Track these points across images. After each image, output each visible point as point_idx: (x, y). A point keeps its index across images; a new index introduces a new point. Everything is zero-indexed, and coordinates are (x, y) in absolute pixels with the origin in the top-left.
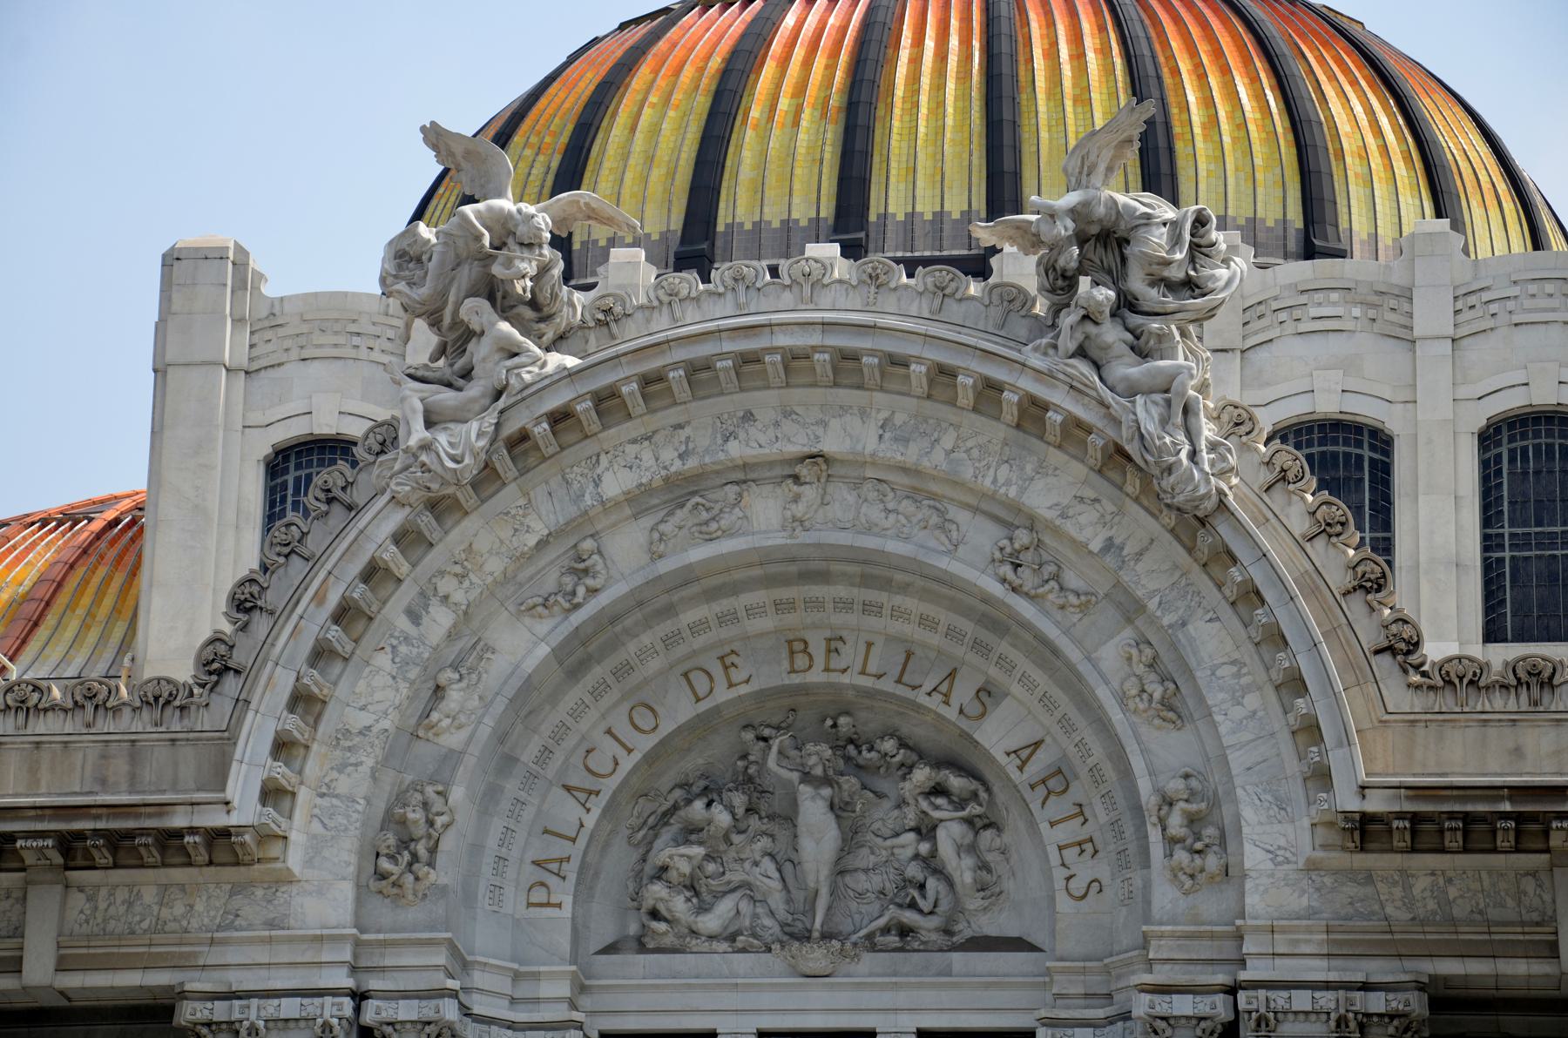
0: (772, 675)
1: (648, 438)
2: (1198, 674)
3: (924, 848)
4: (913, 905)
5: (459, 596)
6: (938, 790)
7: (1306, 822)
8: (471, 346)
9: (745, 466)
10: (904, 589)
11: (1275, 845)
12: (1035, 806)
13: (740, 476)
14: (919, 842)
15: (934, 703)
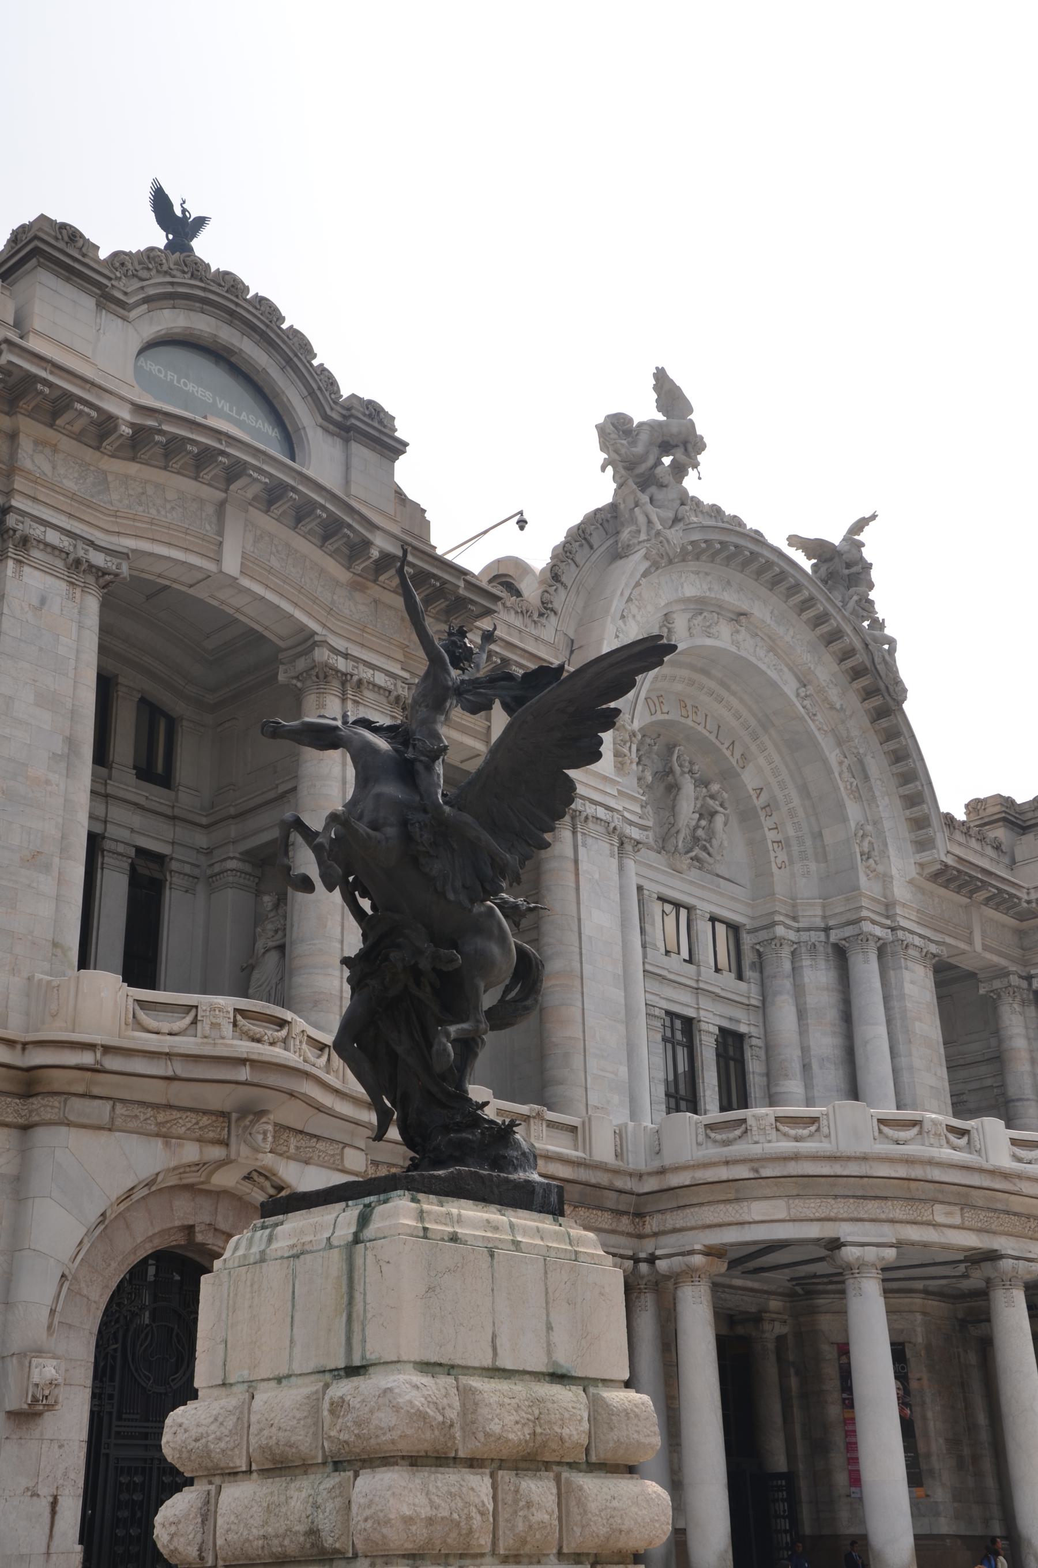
0: (674, 716)
1: (697, 573)
2: (873, 781)
3: (703, 823)
4: (704, 849)
5: (638, 618)
6: (712, 797)
7: (912, 861)
8: (653, 489)
9: (720, 607)
10: (734, 694)
11: (902, 868)
12: (762, 818)
13: (718, 610)
14: (699, 820)
15: (728, 753)
